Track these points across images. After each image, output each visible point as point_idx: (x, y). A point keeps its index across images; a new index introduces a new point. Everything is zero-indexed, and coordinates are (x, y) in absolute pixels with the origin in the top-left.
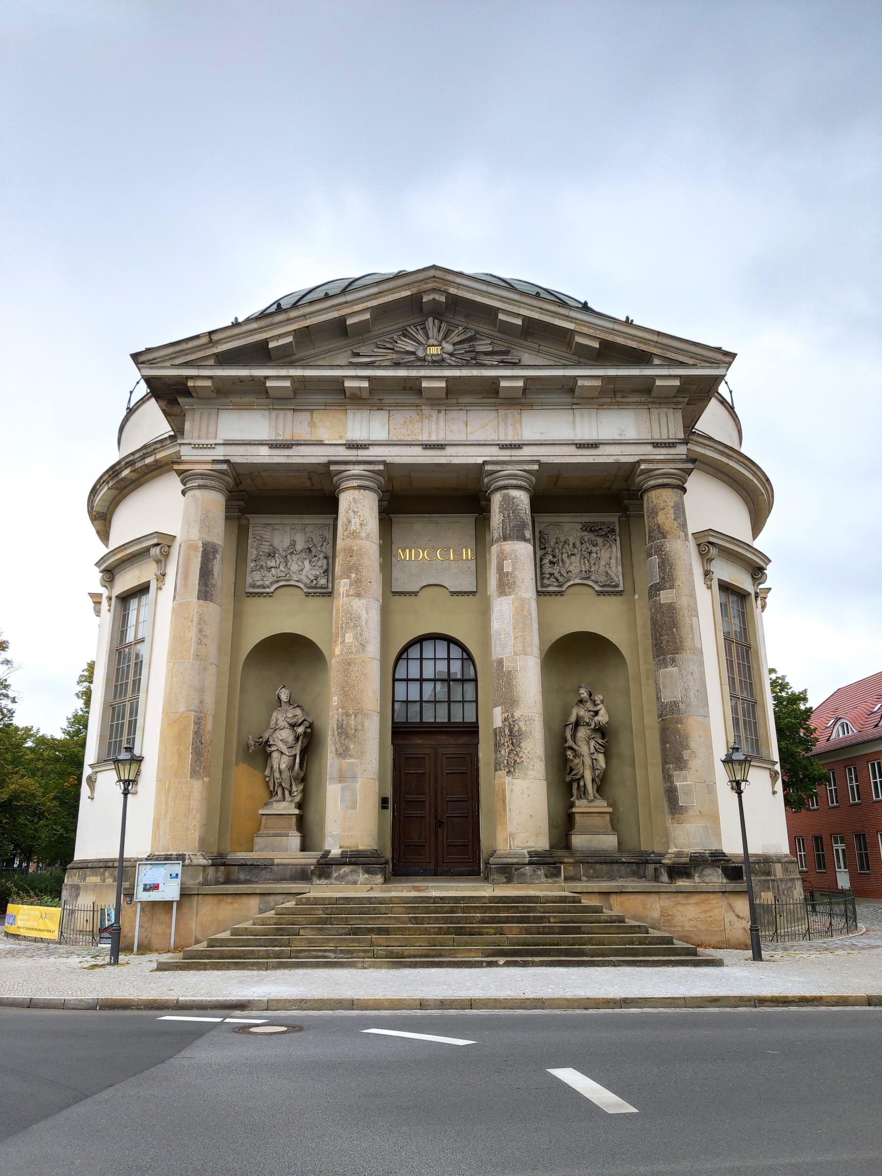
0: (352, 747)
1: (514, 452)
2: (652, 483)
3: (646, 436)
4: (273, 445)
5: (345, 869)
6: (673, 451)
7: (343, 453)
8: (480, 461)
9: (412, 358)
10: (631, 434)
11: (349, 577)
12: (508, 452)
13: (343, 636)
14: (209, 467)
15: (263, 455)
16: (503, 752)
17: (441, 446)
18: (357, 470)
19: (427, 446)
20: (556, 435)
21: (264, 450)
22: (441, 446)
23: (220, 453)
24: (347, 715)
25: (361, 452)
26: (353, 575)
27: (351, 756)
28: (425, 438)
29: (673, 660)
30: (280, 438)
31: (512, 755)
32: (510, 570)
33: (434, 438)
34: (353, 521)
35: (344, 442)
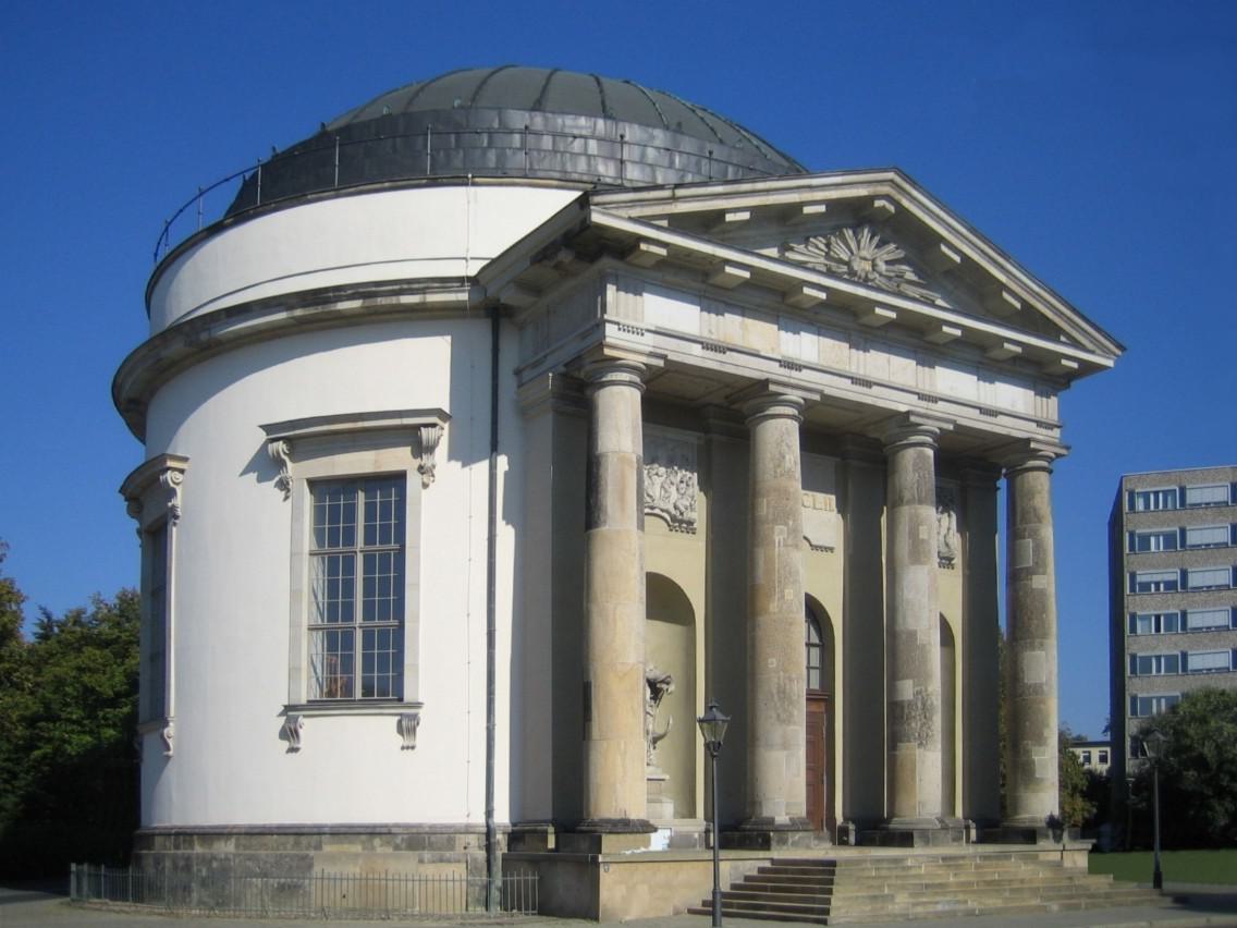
0: (796, 713)
1: (931, 405)
2: (1031, 463)
3: (1030, 413)
4: (707, 346)
5: (797, 836)
6: (1049, 432)
7: (773, 371)
8: (903, 408)
9: (844, 269)
10: (1020, 409)
11: (786, 524)
12: (924, 404)
13: (782, 592)
14: (644, 359)
15: (695, 356)
16: (913, 725)
17: (868, 384)
18: (795, 395)
19: (855, 380)
20: (961, 395)
21: (697, 349)
22: (868, 384)
23: (649, 342)
24: (791, 680)
25: (794, 373)
26: (791, 523)
27: (795, 723)
28: (853, 370)
29: (1042, 644)
30: (713, 337)
31: (924, 729)
32: (925, 537)
33: (861, 372)
34: (787, 457)
35: (779, 358)
